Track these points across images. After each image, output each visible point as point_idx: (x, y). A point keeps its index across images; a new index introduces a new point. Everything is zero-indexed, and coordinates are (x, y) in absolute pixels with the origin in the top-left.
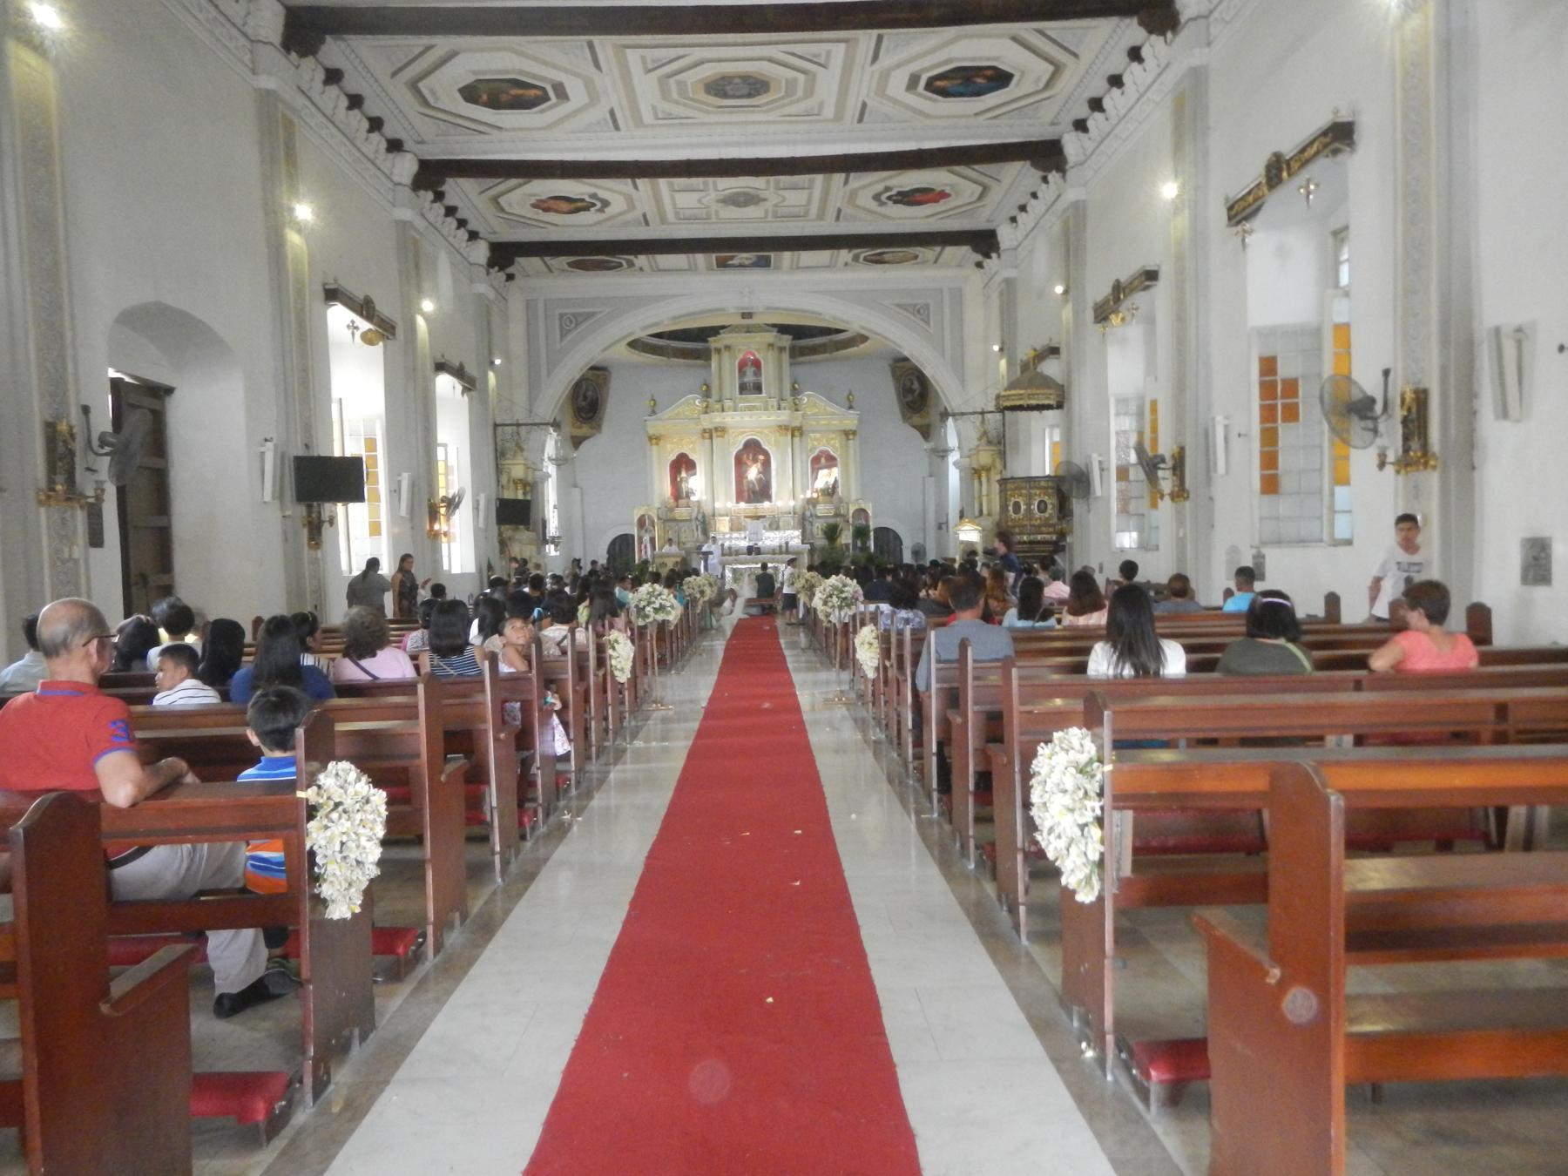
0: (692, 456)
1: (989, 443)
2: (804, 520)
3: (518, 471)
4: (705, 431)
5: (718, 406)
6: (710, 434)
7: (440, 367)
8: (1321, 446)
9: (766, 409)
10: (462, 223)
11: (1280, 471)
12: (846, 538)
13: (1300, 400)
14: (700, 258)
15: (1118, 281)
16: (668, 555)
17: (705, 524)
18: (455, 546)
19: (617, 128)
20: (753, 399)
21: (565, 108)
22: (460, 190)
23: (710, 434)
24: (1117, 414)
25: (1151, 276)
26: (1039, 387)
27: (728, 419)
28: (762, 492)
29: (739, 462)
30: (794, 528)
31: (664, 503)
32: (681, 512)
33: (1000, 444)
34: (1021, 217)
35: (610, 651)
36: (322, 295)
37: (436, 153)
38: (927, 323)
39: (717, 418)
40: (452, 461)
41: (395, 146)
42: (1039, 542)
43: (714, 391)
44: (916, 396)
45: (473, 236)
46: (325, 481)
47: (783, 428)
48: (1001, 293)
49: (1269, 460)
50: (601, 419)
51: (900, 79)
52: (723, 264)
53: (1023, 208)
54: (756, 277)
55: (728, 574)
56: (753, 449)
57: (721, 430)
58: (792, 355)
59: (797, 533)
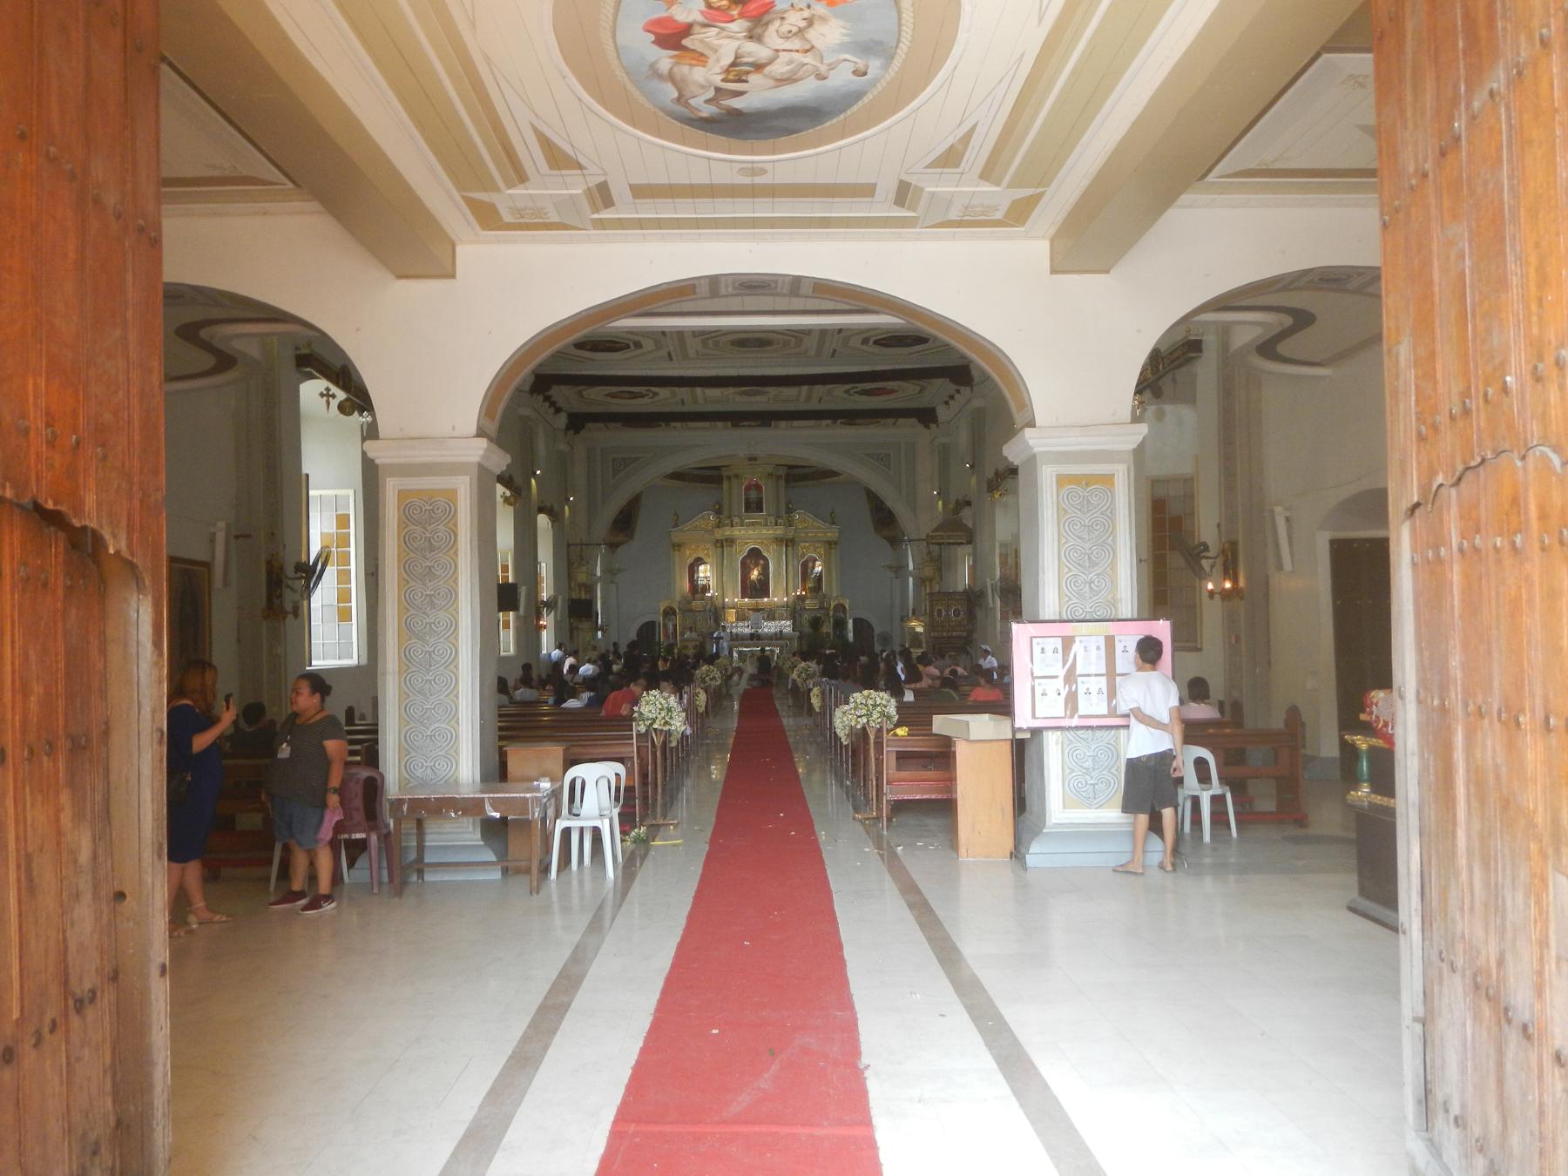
3: (582, 577)
6: (724, 544)
7: (541, 510)
10: (553, 404)
12: (827, 628)
14: (720, 424)
17: (717, 613)
18: (544, 633)
21: (639, 351)
23: (724, 544)
26: (958, 528)
28: (761, 588)
29: (743, 563)
31: (684, 597)
32: (697, 604)
33: (939, 564)
39: (728, 532)
44: (884, 519)
45: (558, 410)
47: (778, 540)
52: (735, 425)
53: (952, 397)
56: (755, 555)
57: (731, 541)
58: (787, 482)
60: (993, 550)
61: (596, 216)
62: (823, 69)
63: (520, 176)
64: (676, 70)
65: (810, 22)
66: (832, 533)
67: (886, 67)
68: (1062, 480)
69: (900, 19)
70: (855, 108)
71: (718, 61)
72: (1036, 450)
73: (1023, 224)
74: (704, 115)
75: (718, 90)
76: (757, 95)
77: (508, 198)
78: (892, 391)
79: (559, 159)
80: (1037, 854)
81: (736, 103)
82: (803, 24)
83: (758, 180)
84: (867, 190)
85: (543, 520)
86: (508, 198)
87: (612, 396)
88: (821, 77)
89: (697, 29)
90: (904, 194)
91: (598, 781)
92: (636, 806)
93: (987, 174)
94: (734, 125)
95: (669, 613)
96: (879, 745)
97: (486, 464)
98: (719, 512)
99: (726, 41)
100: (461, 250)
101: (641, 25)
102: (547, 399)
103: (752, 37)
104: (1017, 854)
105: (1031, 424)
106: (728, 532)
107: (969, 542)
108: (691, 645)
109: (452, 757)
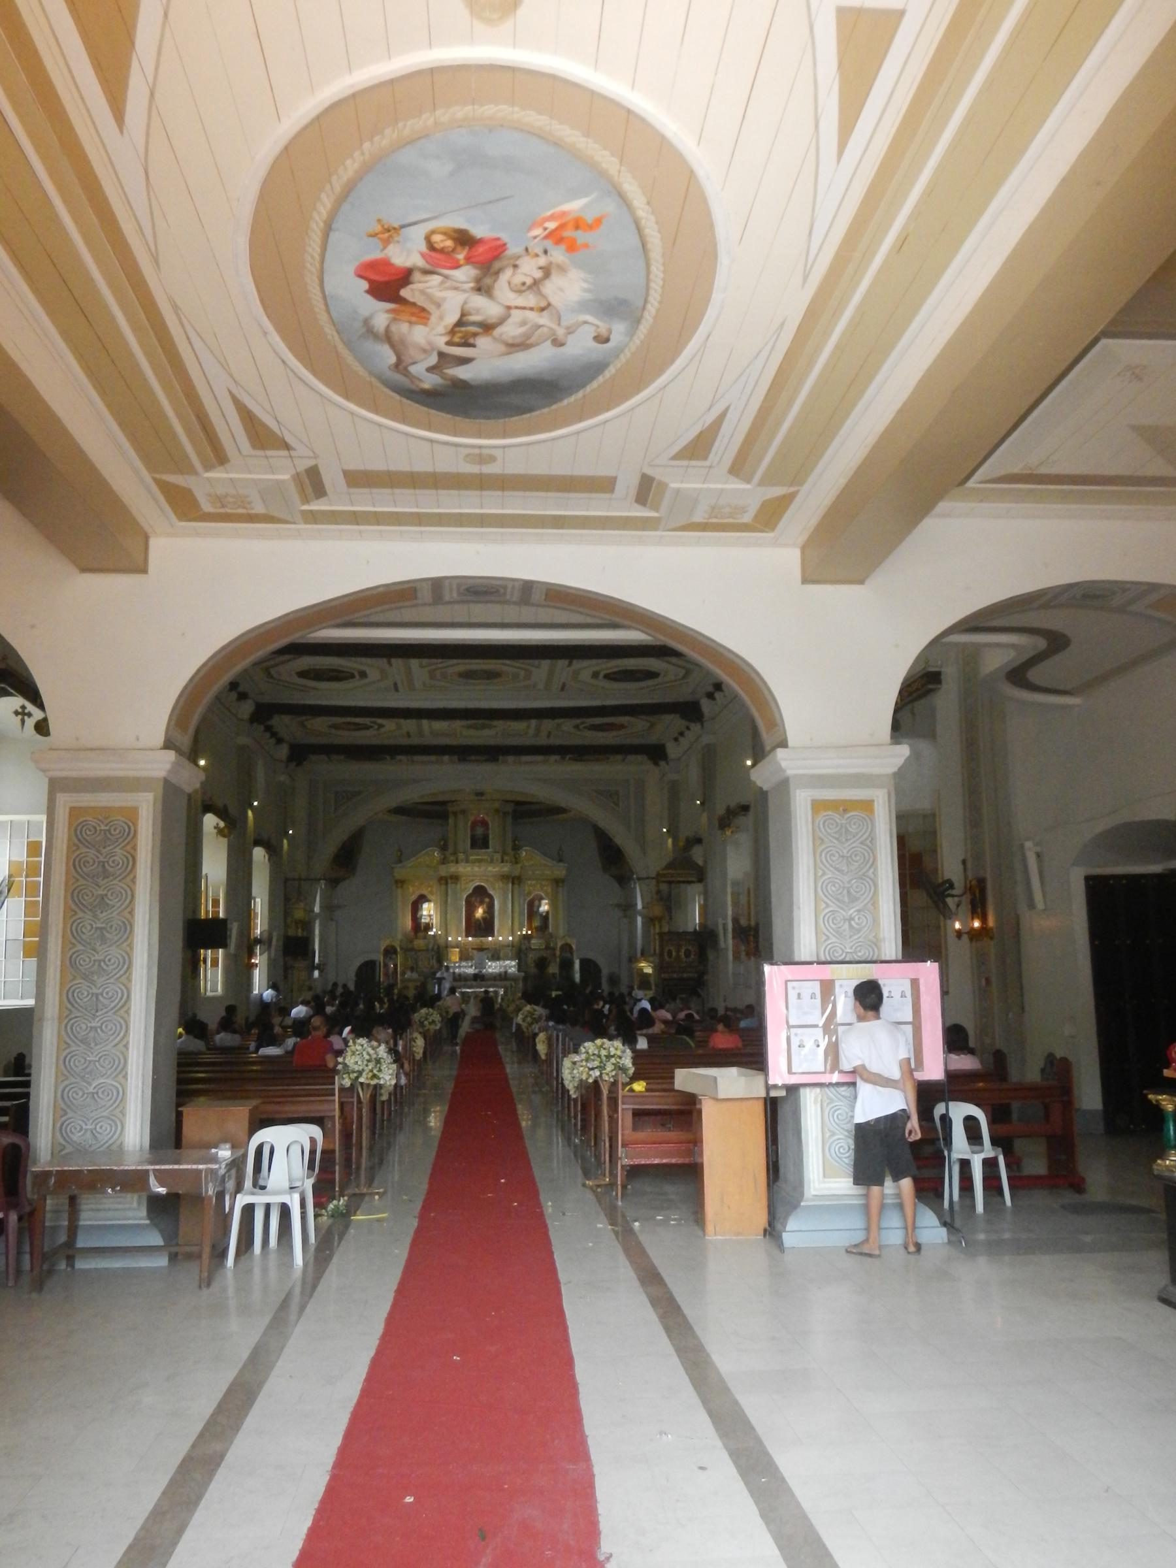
1: (661, 899)
3: (299, 914)
5: (452, 858)
7: (257, 843)
9: (492, 861)
10: (274, 734)
12: (553, 969)
16: (410, 980)
18: (257, 972)
19: (396, 689)
20: (482, 854)
22: (281, 723)
25: (745, 808)
26: (688, 868)
28: (485, 927)
30: (512, 959)
32: (419, 943)
34: (681, 739)
37: (266, 699)
38: (617, 805)
39: (453, 869)
40: (259, 910)
44: (612, 858)
45: (280, 741)
47: (504, 878)
51: (586, 675)
52: (463, 760)
53: (682, 734)
54: (488, 768)
57: (455, 878)
60: (725, 886)
61: (305, 507)
62: (560, 332)
63: (220, 458)
64: (394, 328)
65: (547, 272)
66: (560, 871)
67: (631, 333)
68: (818, 806)
69: (648, 273)
70: (595, 384)
71: (441, 318)
72: (789, 772)
73: (773, 529)
74: (426, 386)
75: (441, 355)
76: (487, 363)
77: (207, 483)
78: (622, 727)
79: (262, 437)
80: (795, 1232)
81: (463, 373)
82: (538, 274)
83: (488, 469)
84: (605, 485)
85: (259, 853)
86: (207, 483)
87: (335, 726)
88: (558, 343)
89: (417, 276)
90: (646, 490)
91: (289, 1147)
92: (331, 1175)
93: (739, 468)
94: (460, 400)
95: (390, 952)
96: (613, 1101)
97: (174, 780)
98: (444, 848)
99: (448, 294)
100: (154, 543)
101: (351, 269)
102: (268, 729)
103: (482, 288)
104: (772, 1231)
105: (784, 744)
107: (700, 880)
108: (411, 985)
109: (117, 1117)
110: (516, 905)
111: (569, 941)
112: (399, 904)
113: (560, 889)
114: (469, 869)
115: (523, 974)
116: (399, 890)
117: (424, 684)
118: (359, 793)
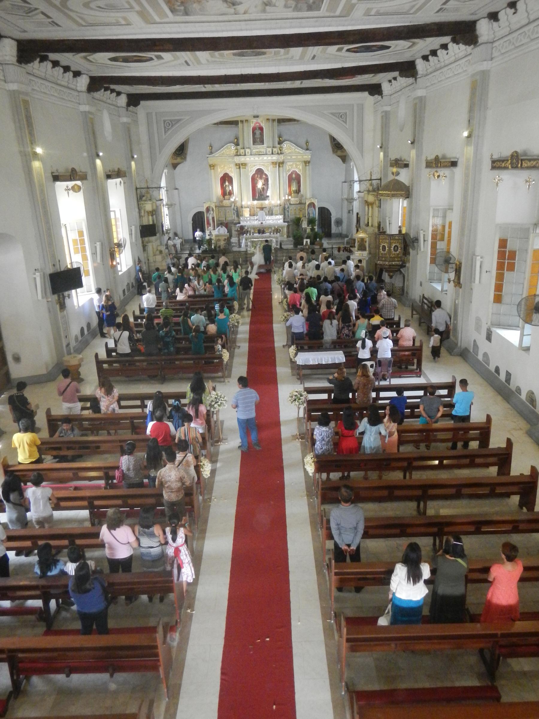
0: (231, 175)
2: (284, 210)
3: (148, 207)
4: (236, 165)
8: (523, 284)
11: (503, 293)
12: (304, 225)
13: (516, 261)
15: (437, 156)
17: (238, 213)
23: (239, 166)
24: (433, 217)
27: (248, 159)
31: (218, 198)
35: (201, 469)
36: (51, 179)
38: (346, 122)
39: (242, 159)
40: (118, 216)
41: (77, 74)
42: (393, 265)
43: (241, 142)
46: (65, 280)
47: (274, 163)
48: (382, 117)
49: (499, 288)
50: (186, 154)
55: (249, 244)
56: (260, 172)
57: (244, 165)
59: (281, 217)
66: (307, 156)
98: (237, 144)
106: (242, 159)
110: (281, 175)
111: (313, 201)
112: (213, 179)
113: (307, 167)
114: (252, 159)
115: (286, 224)
116: (212, 171)
117: (208, 61)
118: (178, 121)
